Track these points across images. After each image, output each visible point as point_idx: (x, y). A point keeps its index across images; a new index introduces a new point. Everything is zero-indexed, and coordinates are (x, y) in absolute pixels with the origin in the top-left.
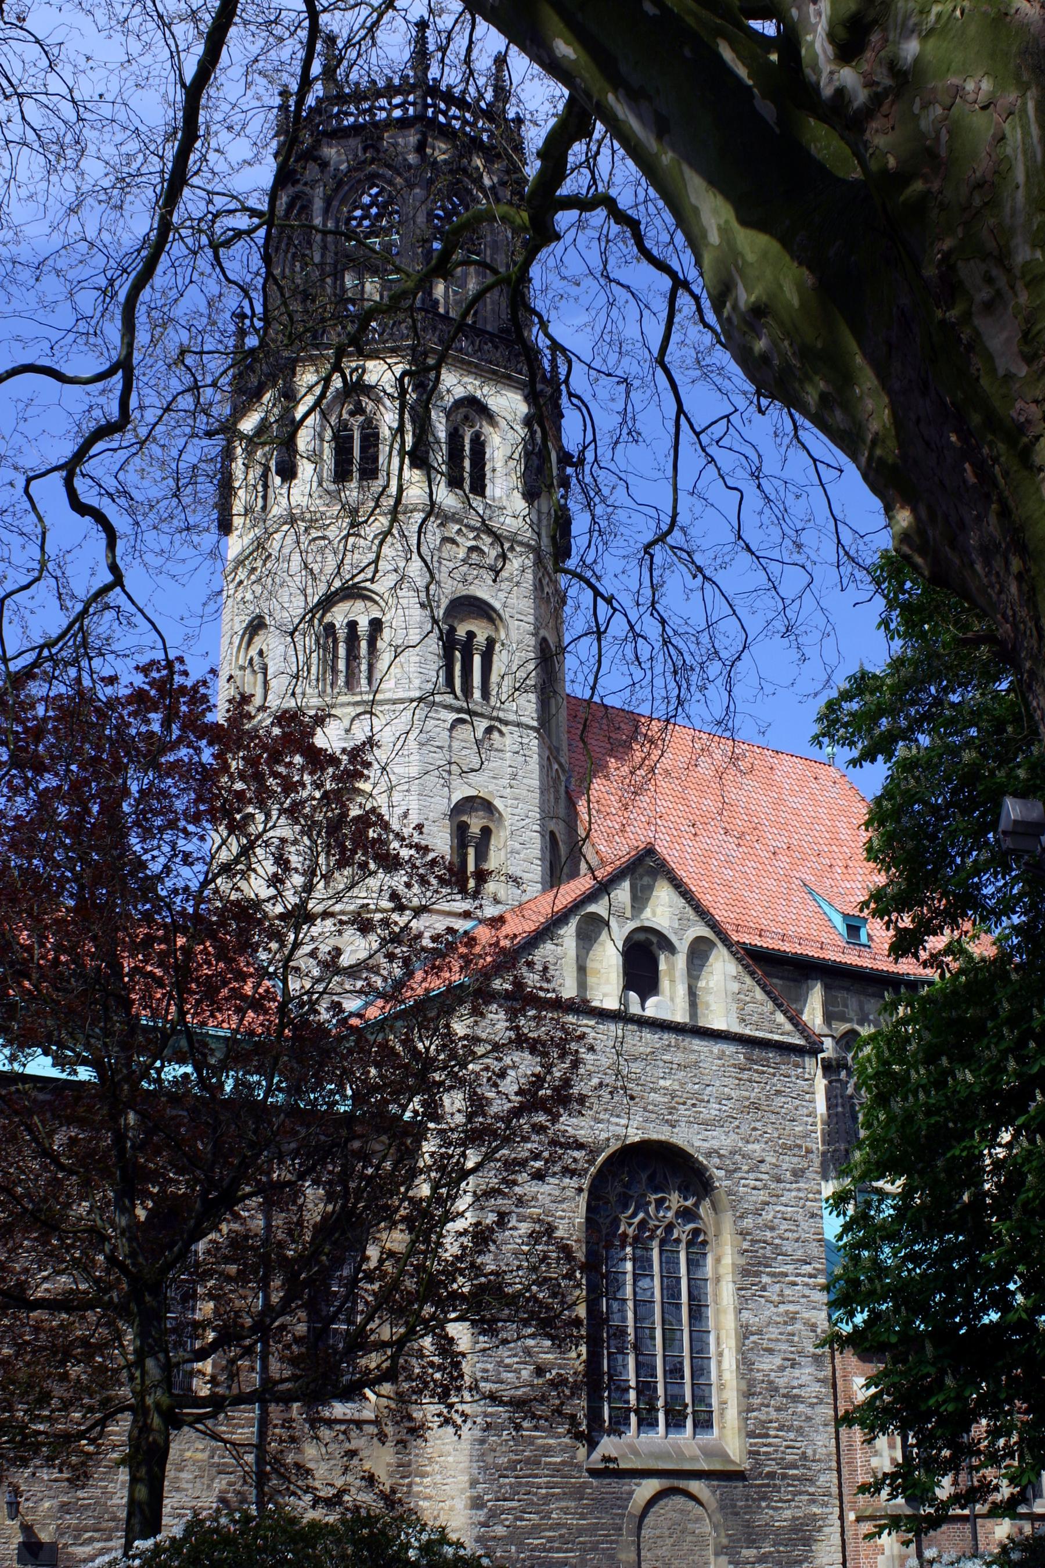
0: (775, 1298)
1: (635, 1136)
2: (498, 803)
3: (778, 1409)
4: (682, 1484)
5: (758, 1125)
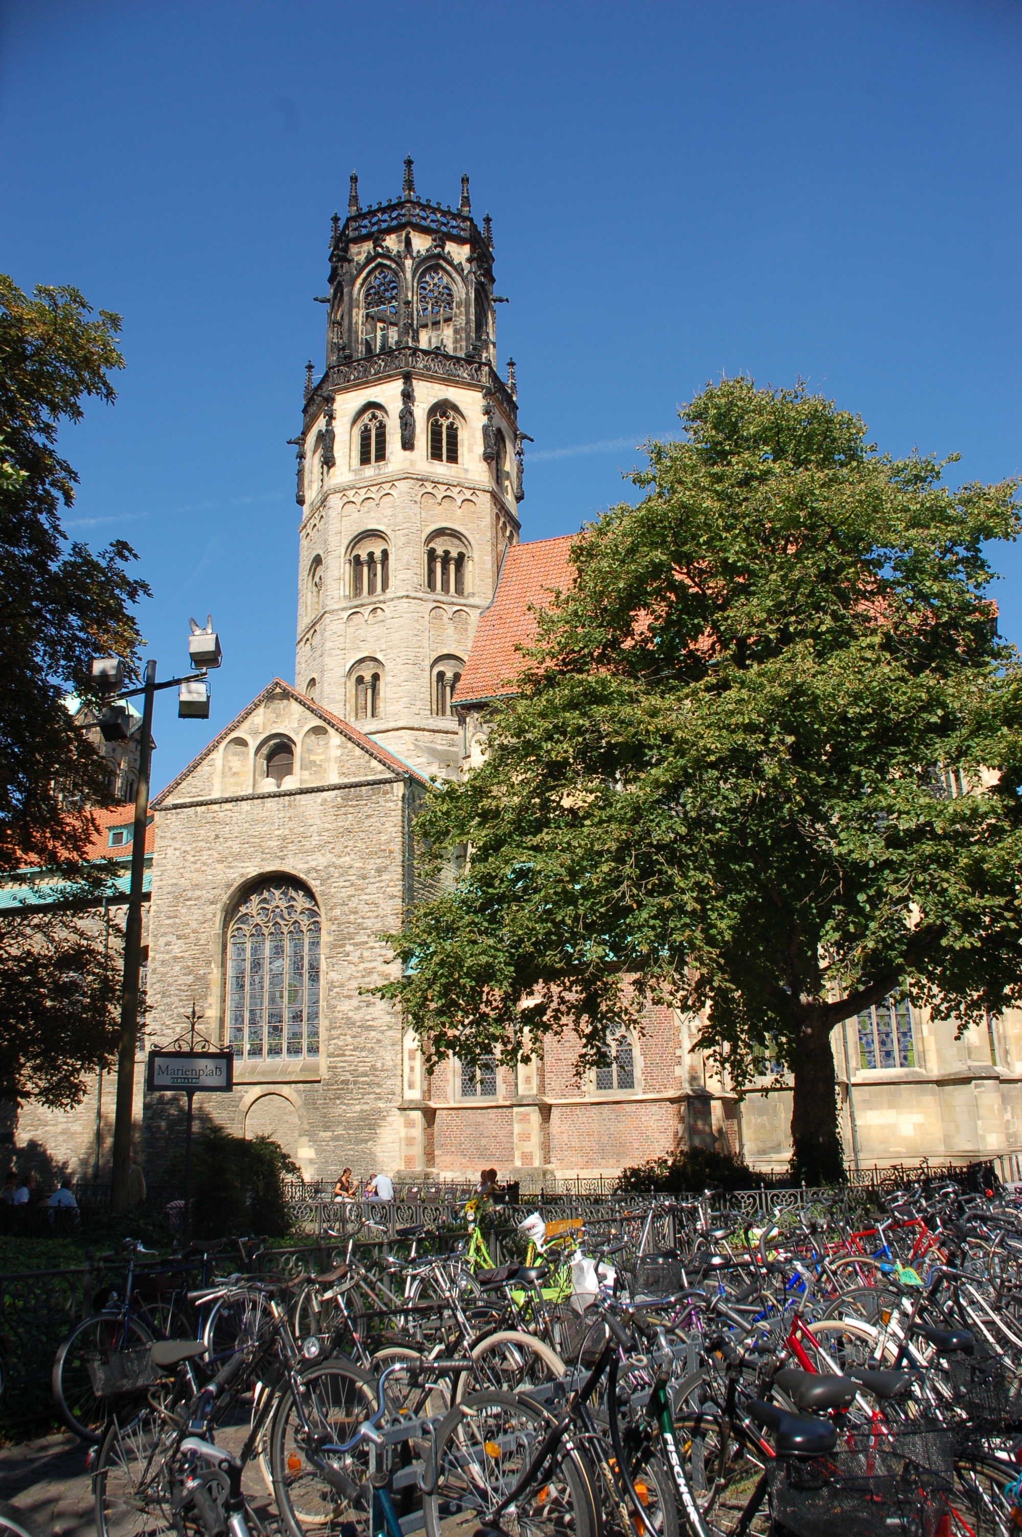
0: (356, 960)
2: (379, 656)
3: (354, 1037)
5: (350, 843)
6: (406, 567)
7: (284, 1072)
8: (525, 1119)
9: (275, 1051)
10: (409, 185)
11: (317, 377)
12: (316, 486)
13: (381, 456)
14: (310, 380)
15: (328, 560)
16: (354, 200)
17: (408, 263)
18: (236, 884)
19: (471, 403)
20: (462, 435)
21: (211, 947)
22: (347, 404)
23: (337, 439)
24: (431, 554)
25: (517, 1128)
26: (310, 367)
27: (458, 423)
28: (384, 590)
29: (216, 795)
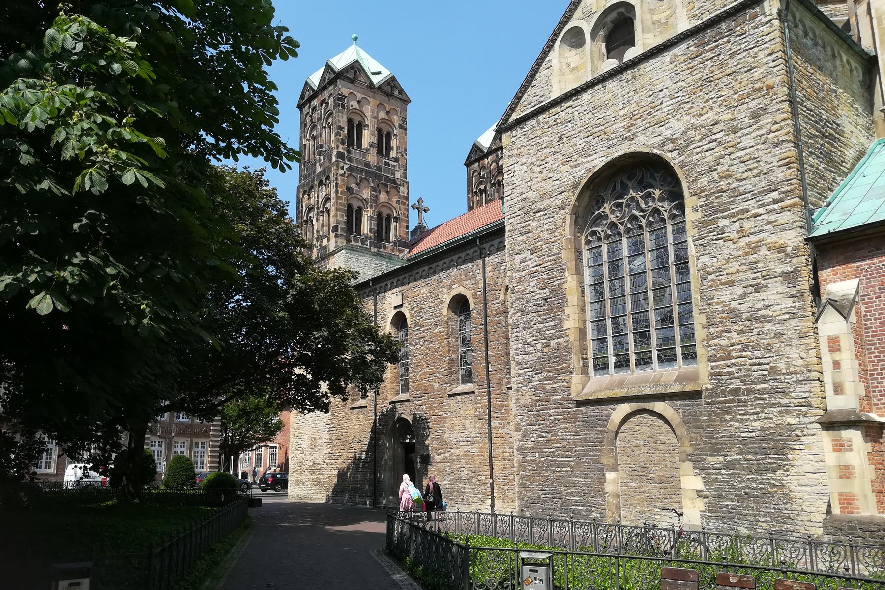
0: (734, 236)
1: (598, 162)
3: (740, 333)
7: (657, 382)
9: (644, 361)
18: (583, 182)
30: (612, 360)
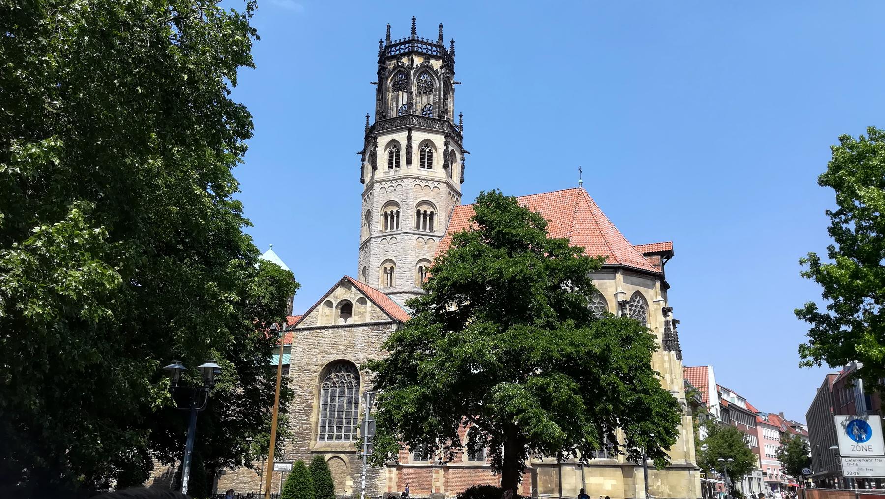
1: (333, 359)
4: (338, 455)
6: (408, 220)
7: (342, 446)
8: (437, 472)
9: (339, 438)
10: (414, 31)
11: (372, 122)
12: (370, 175)
13: (398, 166)
14: (367, 123)
15: (374, 214)
16: (388, 37)
17: (412, 72)
19: (439, 140)
20: (434, 155)
21: (314, 391)
22: (383, 140)
23: (378, 156)
24: (418, 212)
25: (434, 476)
26: (368, 117)
27: (433, 150)
28: (397, 227)
29: (318, 325)
30: (327, 436)
